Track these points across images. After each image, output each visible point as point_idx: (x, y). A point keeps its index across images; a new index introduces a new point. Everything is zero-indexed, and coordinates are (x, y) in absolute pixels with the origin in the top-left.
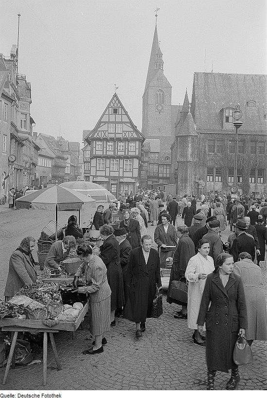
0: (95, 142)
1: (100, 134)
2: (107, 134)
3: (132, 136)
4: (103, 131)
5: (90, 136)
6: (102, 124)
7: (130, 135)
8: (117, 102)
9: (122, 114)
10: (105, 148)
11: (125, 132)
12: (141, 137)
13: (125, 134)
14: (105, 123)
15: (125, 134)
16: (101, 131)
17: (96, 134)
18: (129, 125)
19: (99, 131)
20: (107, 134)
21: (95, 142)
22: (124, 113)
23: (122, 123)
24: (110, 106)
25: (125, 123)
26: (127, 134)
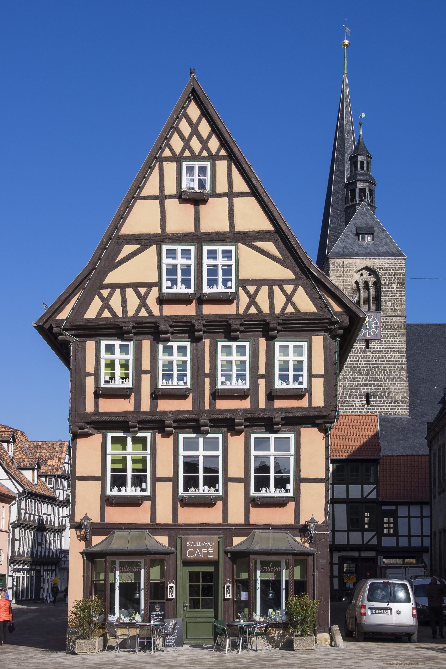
0: (90, 345)
1: (116, 302)
2: (151, 301)
3: (290, 309)
4: (135, 286)
5: (64, 314)
6: (128, 249)
7: (280, 300)
8: (205, 128)
9: (231, 195)
10: (146, 380)
11: (252, 289)
12: (337, 308)
13: (252, 298)
14: (144, 241)
15: (252, 298)
16: (123, 287)
17: (97, 303)
18: (270, 247)
19: (113, 287)
20: (151, 301)
21: (90, 345)
22: (240, 185)
23: (232, 237)
24: (167, 153)
25: (249, 238)
26: (262, 299)
